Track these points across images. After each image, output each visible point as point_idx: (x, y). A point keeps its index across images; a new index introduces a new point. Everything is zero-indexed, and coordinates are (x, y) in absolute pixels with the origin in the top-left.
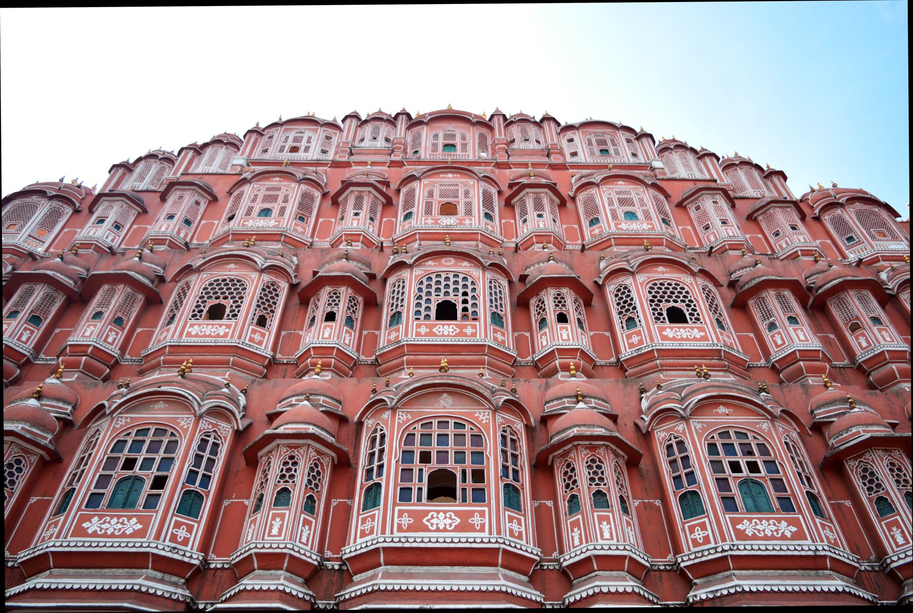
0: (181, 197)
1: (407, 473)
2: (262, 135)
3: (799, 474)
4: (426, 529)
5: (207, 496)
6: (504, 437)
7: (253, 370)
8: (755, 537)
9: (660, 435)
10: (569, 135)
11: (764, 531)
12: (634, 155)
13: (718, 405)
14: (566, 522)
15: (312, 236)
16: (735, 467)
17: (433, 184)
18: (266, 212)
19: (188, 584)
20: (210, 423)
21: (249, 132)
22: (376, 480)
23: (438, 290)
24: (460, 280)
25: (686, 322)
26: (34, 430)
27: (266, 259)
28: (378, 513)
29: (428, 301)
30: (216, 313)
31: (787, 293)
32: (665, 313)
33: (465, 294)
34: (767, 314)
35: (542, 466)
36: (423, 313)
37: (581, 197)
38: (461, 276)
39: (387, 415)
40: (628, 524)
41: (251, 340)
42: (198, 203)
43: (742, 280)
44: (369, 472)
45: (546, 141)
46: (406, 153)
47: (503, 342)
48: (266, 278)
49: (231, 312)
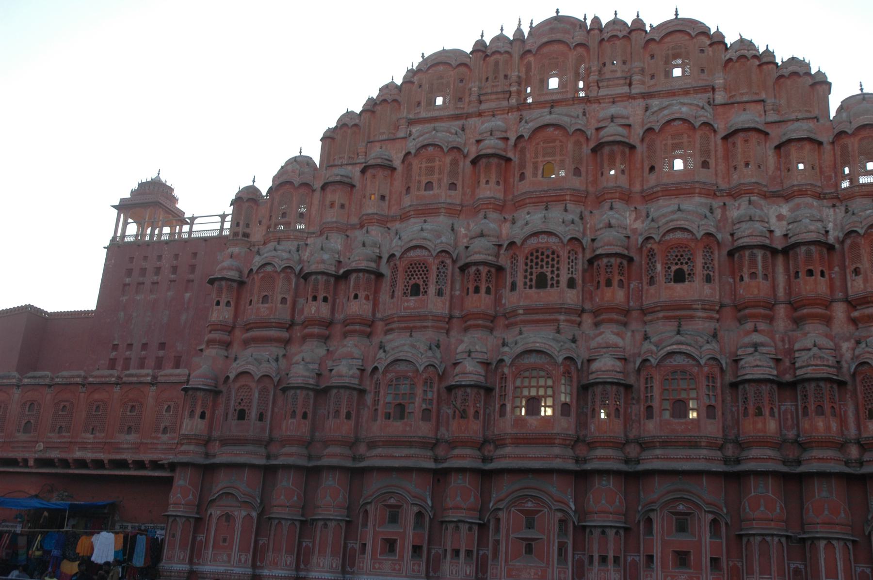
2: (412, 83)
7: (442, 328)
18: (429, 186)
19: (432, 449)
23: (537, 264)
30: (415, 290)
32: (672, 274)
33: (553, 266)
34: (741, 270)
36: (529, 283)
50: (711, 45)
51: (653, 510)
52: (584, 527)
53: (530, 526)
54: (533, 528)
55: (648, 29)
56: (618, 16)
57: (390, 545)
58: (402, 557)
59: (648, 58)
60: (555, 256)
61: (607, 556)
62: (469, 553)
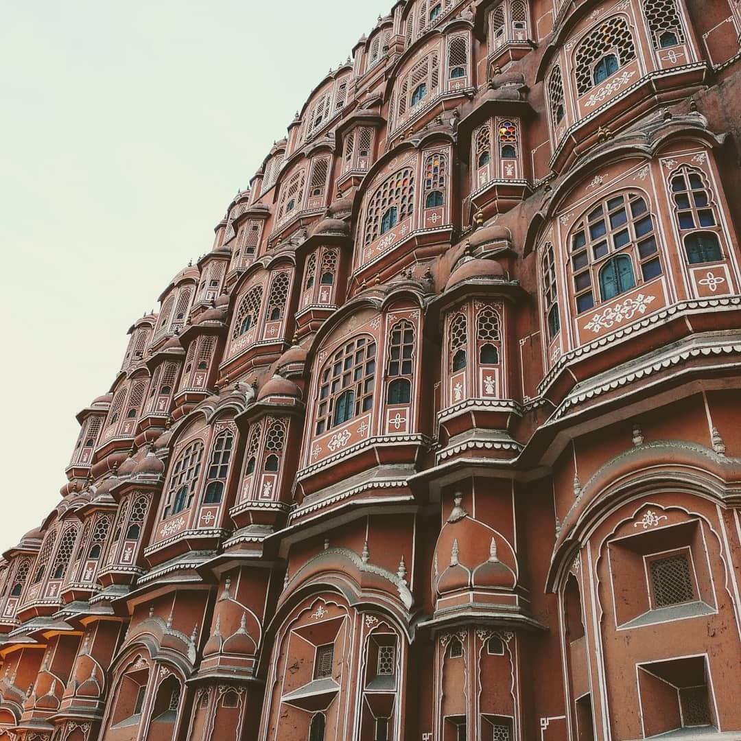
5: (225, 482)
6: (396, 335)
8: (603, 331)
11: (614, 318)
13: (591, 178)
17: (407, 76)
20: (222, 424)
21: (289, 129)
26: (148, 475)
27: (273, 256)
32: (591, 76)
38: (403, 172)
40: (486, 374)
41: (268, 335)
46: (402, 50)
47: (439, 221)
48: (275, 273)
53: (323, 669)
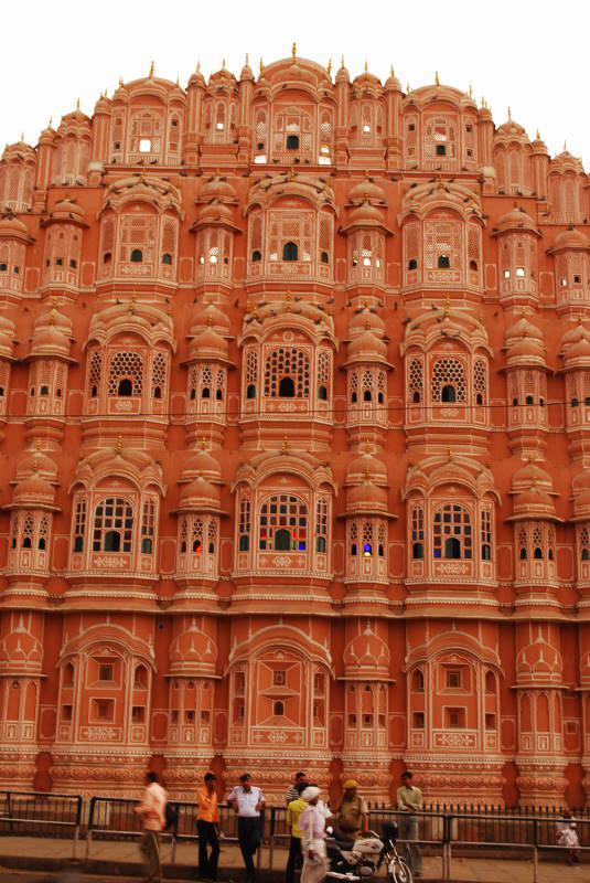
0: (62, 236)
1: (263, 532)
2: (109, 116)
3: (483, 534)
4: (275, 566)
9: (411, 503)
10: (412, 119)
12: (469, 153)
14: (349, 558)
15: (177, 281)
16: (447, 530)
18: (137, 256)
22: (246, 533)
23: (281, 367)
24: (297, 355)
25: (454, 400)
28: (249, 554)
29: (274, 378)
30: (125, 389)
31: (537, 375)
32: (441, 392)
33: (300, 371)
35: (340, 521)
37: (406, 227)
38: (298, 352)
39: (249, 489)
42: (75, 238)
43: (508, 353)
44: (242, 527)
45: (387, 134)
49: (136, 387)
50: (478, 124)
51: (424, 663)
52: (343, 683)
54: (284, 684)
55: (404, 91)
56: (369, 71)
57: (104, 708)
58: (120, 723)
59: (406, 125)
60: (303, 359)
61: (372, 716)
62: (205, 715)
